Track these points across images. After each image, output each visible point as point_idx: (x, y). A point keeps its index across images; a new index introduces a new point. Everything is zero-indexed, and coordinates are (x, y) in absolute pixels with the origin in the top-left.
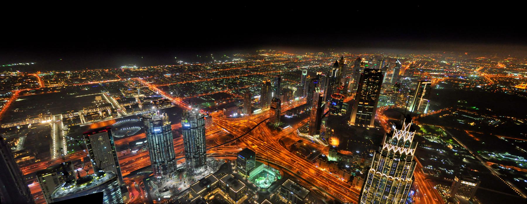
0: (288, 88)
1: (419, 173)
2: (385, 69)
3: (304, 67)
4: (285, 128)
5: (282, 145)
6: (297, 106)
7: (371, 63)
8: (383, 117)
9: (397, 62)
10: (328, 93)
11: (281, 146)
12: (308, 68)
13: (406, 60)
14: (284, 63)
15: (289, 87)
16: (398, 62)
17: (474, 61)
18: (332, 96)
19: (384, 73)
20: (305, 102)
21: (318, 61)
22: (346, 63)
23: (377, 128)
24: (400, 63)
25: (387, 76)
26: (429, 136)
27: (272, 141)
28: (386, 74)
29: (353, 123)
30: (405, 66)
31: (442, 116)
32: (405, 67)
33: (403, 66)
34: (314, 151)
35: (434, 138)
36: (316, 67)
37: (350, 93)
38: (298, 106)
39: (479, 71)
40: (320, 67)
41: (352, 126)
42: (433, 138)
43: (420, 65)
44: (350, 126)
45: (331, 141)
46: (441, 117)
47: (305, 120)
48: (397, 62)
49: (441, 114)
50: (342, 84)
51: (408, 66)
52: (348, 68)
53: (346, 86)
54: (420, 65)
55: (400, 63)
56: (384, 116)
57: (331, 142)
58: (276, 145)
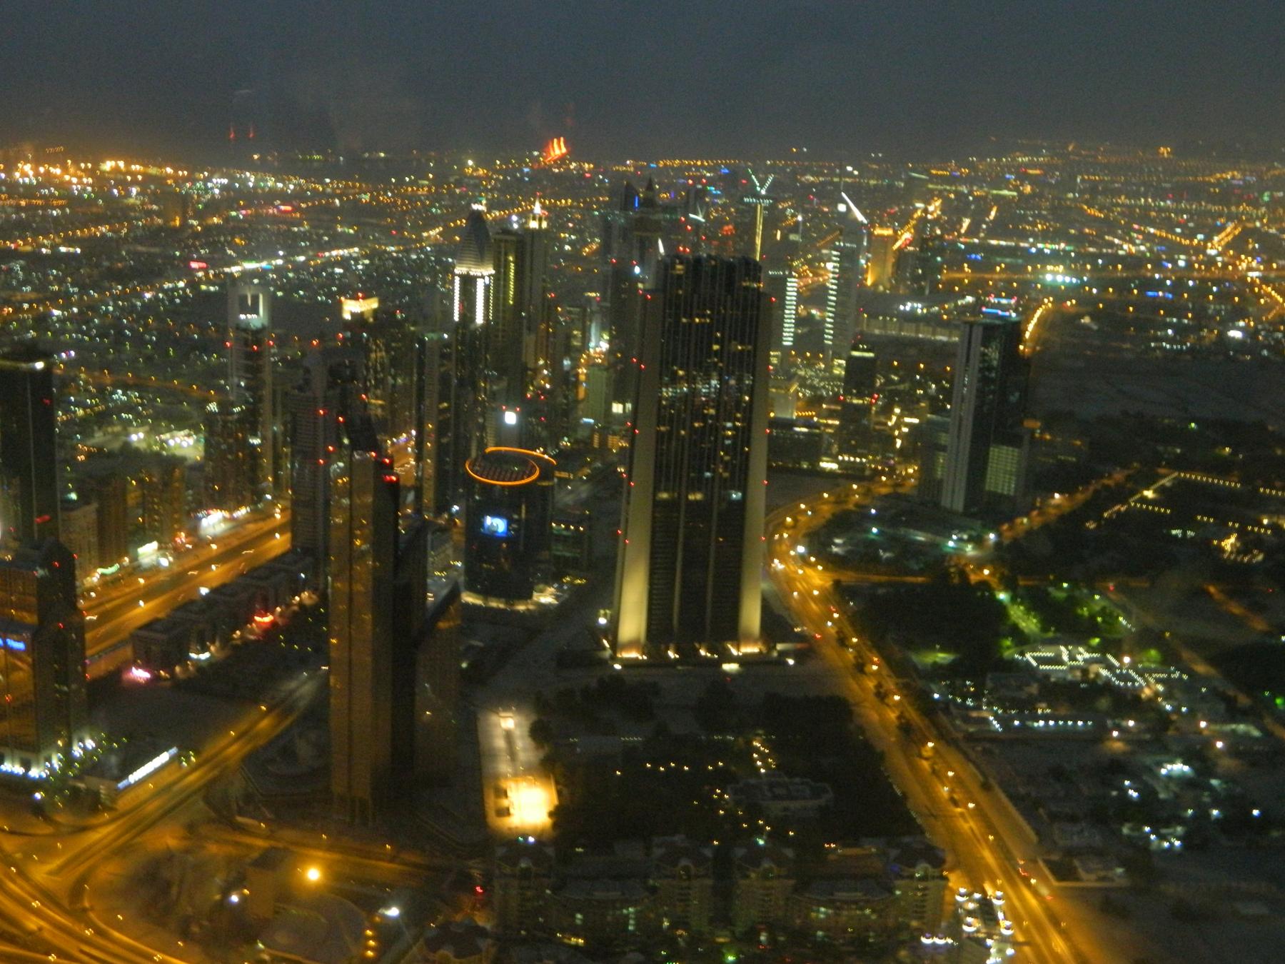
0: (127, 445)
1: (1029, 886)
2: (783, 254)
3: (250, 265)
4: (134, 777)
5: (120, 930)
6: (215, 584)
7: (700, 218)
8: (809, 571)
9: (842, 208)
10: (441, 451)
11: (116, 934)
12: (277, 270)
13: (891, 195)
14: (69, 242)
15: (137, 437)
16: (849, 208)
17: (1196, 192)
18: (472, 466)
19: (780, 284)
20: (280, 542)
21: (355, 212)
22: (544, 225)
23: (784, 654)
24: (860, 217)
25: (801, 299)
26: (1053, 648)
27: (37, 913)
28: (792, 286)
29: (631, 645)
30: (888, 232)
31: (1099, 518)
32: (895, 238)
33: (878, 231)
34: (388, 907)
35: (1079, 657)
36: (343, 262)
37: (596, 438)
38: (226, 580)
39: (1228, 246)
40: (366, 257)
41: (628, 664)
42: (1072, 658)
43: (966, 222)
44: (617, 667)
45: (505, 803)
46: (1091, 525)
47: (293, 685)
48: (842, 208)
49: (1094, 507)
50: (537, 370)
51: (907, 235)
52: (567, 256)
53: (566, 381)
54: (966, 222)
55: (860, 217)
56: (813, 566)
57: (505, 812)
58: (70, 933)
